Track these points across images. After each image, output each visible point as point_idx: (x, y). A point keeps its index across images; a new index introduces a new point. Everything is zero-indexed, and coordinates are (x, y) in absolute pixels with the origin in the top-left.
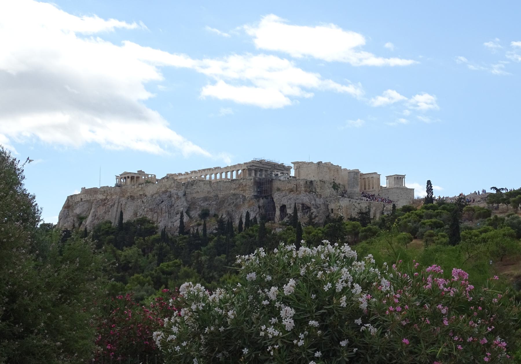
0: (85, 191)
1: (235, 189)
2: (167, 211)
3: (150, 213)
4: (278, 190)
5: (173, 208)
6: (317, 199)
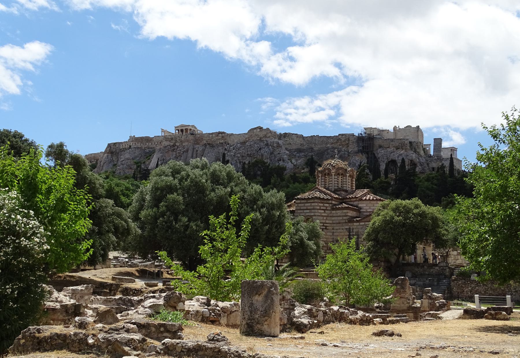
0: (134, 139)
1: (333, 143)
4: (380, 147)
5: (273, 155)
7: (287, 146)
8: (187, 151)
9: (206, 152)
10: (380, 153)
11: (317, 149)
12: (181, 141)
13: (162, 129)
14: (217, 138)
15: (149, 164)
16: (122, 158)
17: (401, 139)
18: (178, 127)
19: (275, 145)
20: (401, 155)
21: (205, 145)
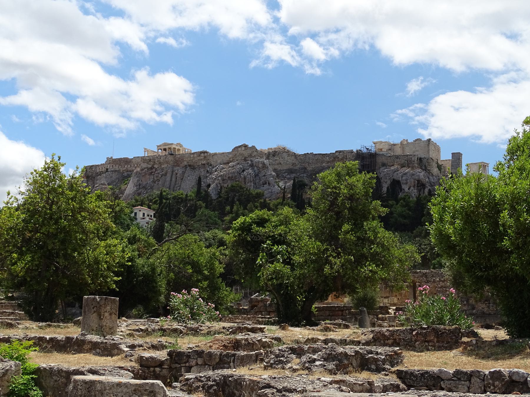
0: (112, 161)
1: (328, 162)
2: (252, 180)
3: (229, 181)
4: (384, 165)
5: (258, 178)
6: (431, 177)
7: (276, 167)
8: (166, 174)
9: (186, 175)
11: (311, 169)
12: (160, 163)
13: (145, 149)
14: (198, 158)
17: (407, 155)
18: (160, 146)
19: (260, 165)
20: (406, 174)
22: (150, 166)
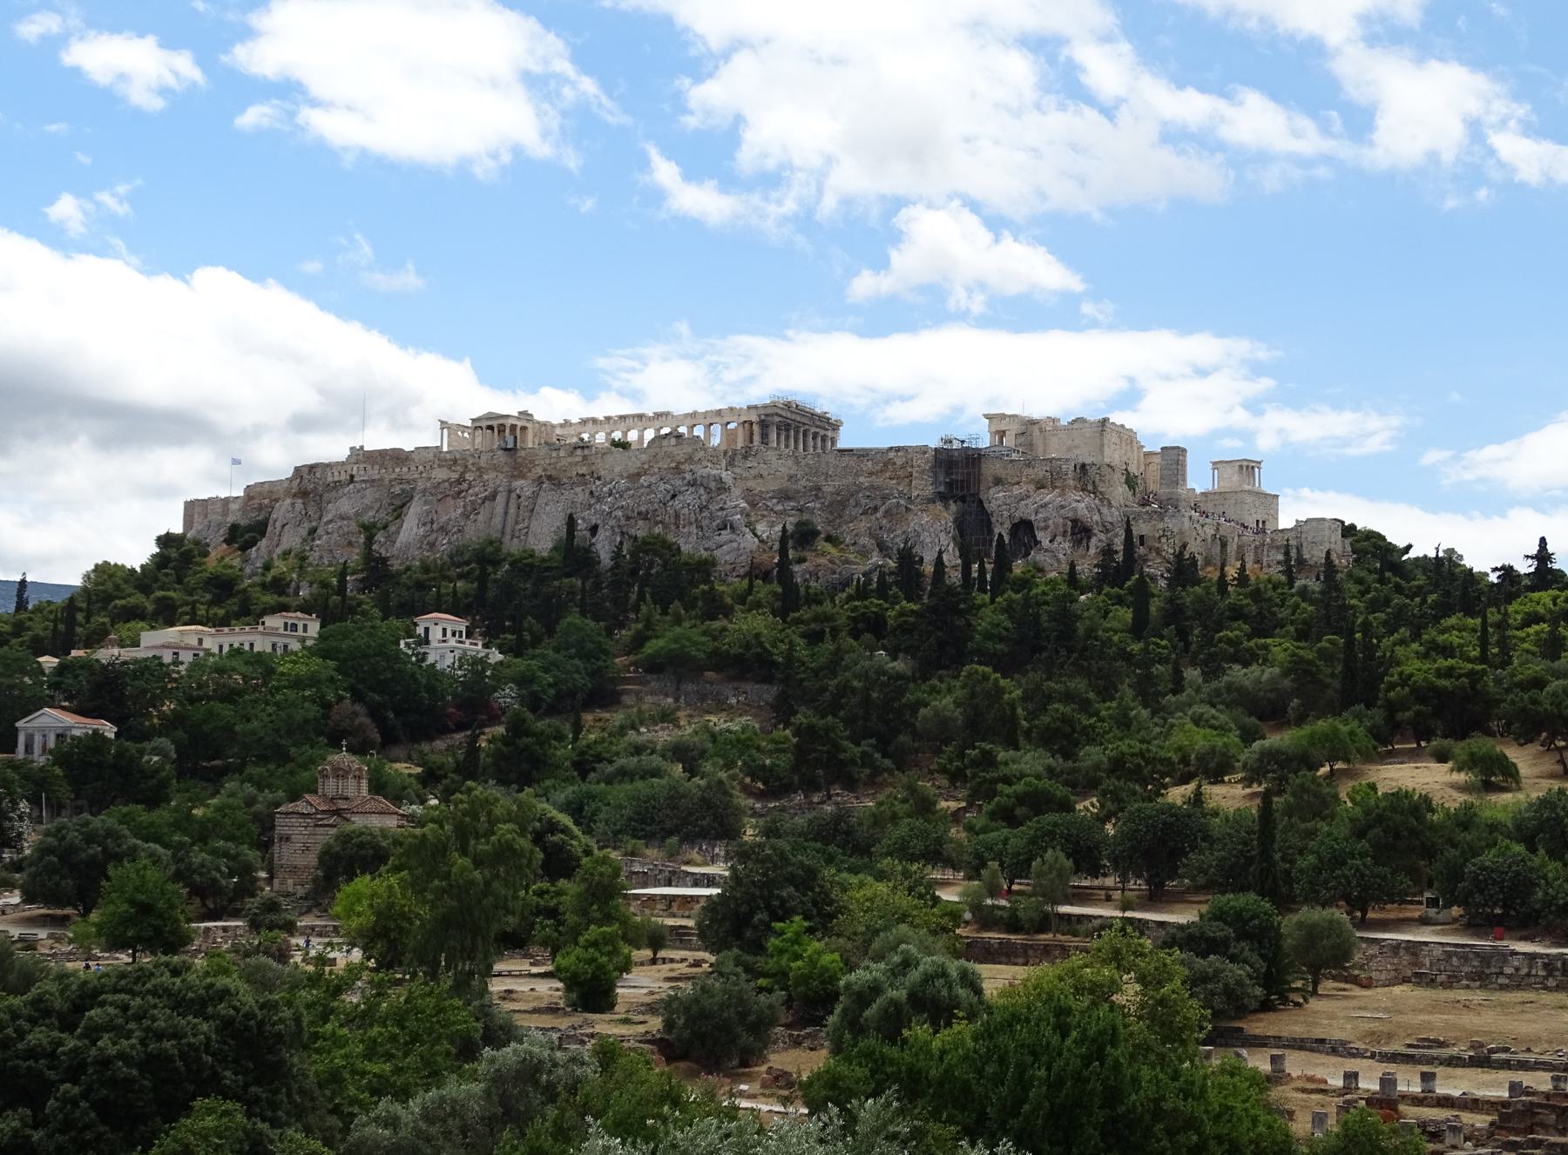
1: (871, 474)
4: (998, 481)
6: (1105, 510)
7: (751, 484)
10: (995, 499)
12: (479, 469)
15: (398, 532)
16: (331, 511)
17: (1051, 460)
19: (713, 485)
20: (1046, 505)
21: (539, 481)
22: (455, 476)
